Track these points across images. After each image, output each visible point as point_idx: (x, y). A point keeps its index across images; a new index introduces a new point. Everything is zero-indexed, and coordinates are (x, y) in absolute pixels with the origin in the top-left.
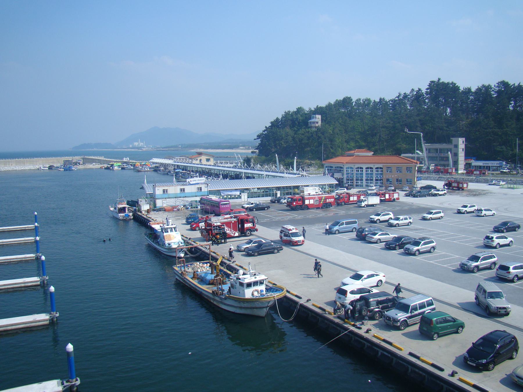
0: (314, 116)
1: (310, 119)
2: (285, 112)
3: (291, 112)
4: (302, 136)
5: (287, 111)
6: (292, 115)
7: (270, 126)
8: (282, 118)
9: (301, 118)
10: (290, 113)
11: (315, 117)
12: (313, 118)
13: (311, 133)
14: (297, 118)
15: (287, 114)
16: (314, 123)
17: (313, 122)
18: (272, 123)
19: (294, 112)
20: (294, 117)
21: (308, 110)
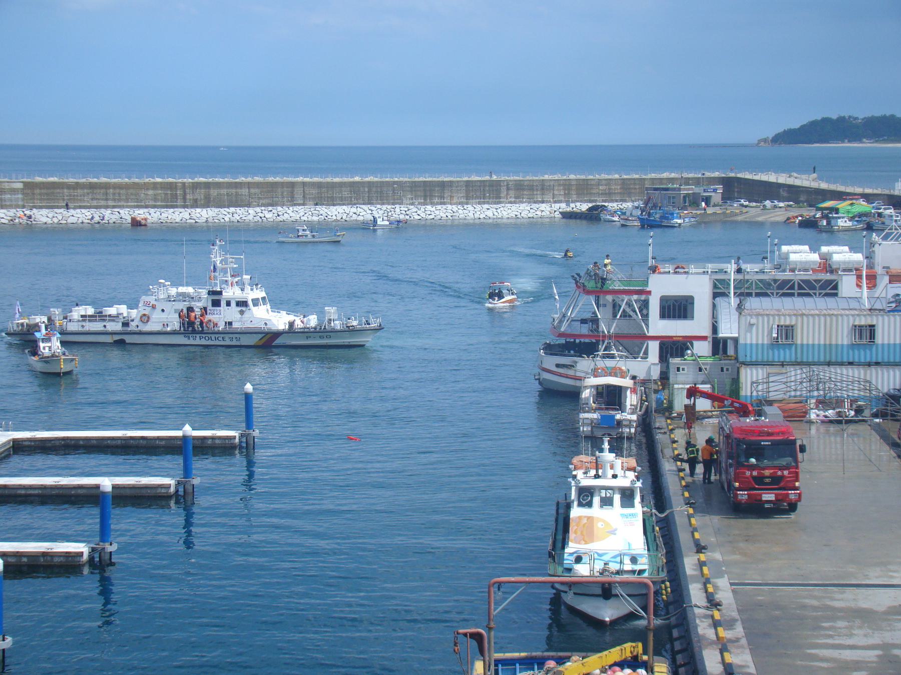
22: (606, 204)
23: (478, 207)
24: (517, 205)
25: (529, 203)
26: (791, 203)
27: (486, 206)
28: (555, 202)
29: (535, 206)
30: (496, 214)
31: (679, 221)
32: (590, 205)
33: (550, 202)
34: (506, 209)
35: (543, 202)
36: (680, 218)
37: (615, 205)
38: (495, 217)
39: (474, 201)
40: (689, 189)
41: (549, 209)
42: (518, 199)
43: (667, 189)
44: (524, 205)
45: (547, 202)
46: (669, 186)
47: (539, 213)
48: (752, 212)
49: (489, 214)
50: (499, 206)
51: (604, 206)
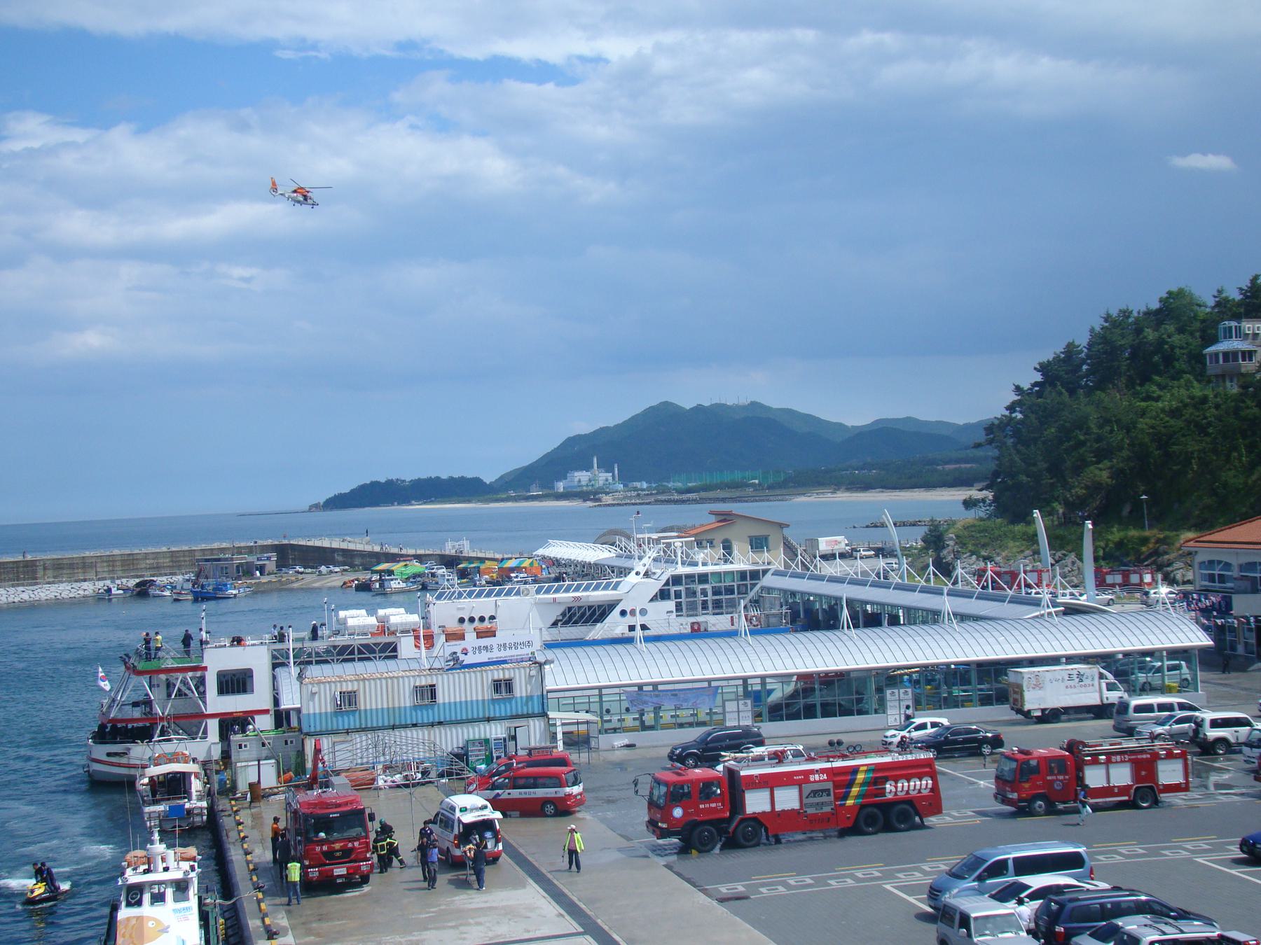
0: (1233, 324)
1: (1214, 340)
2: (1107, 318)
3: (1135, 314)
4: (1172, 422)
5: (1114, 313)
6: (1139, 331)
7: (1036, 384)
8: (1090, 345)
9: (1177, 339)
10: (1130, 320)
11: (1238, 329)
12: (1228, 334)
13: (1217, 407)
14: (1161, 342)
15: (1116, 323)
16: (1229, 356)
17: (1226, 355)
18: (1043, 368)
19: (1148, 313)
20: (1150, 335)
21: (1211, 302)
22: (155, 579)
23: (12, 590)
24: (57, 585)
25: (69, 582)
26: (347, 567)
27: (21, 588)
28: (99, 580)
29: (76, 585)
30: (33, 596)
31: (234, 592)
32: (138, 580)
33: (92, 580)
34: (44, 591)
35: (85, 580)
36: (235, 588)
37: (164, 578)
38: (31, 599)
39: (7, 583)
40: (242, 559)
41: (92, 588)
42: (57, 579)
43: (219, 560)
44: (64, 584)
45: (90, 580)
46: (221, 556)
47: (81, 592)
48: (309, 578)
49: (25, 596)
50: (36, 587)
51: (153, 581)
